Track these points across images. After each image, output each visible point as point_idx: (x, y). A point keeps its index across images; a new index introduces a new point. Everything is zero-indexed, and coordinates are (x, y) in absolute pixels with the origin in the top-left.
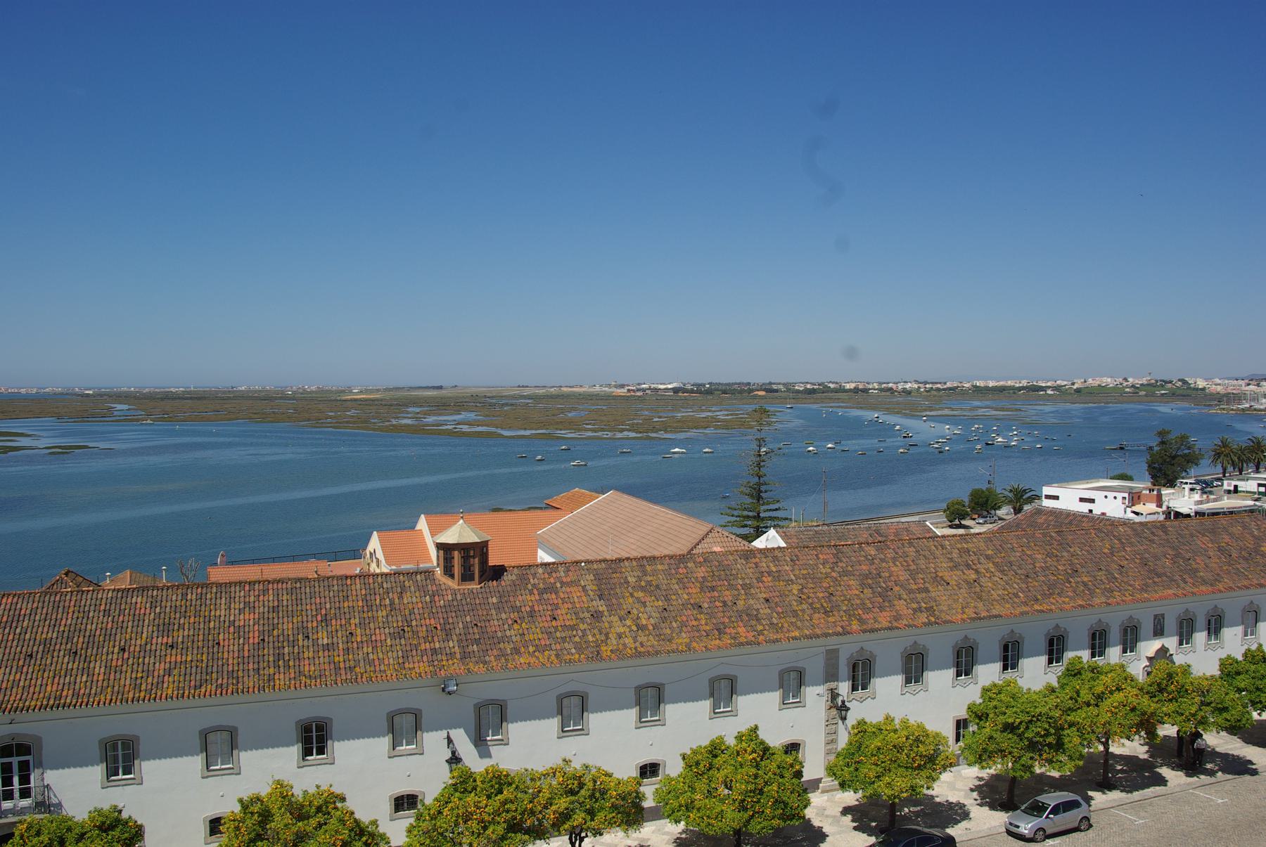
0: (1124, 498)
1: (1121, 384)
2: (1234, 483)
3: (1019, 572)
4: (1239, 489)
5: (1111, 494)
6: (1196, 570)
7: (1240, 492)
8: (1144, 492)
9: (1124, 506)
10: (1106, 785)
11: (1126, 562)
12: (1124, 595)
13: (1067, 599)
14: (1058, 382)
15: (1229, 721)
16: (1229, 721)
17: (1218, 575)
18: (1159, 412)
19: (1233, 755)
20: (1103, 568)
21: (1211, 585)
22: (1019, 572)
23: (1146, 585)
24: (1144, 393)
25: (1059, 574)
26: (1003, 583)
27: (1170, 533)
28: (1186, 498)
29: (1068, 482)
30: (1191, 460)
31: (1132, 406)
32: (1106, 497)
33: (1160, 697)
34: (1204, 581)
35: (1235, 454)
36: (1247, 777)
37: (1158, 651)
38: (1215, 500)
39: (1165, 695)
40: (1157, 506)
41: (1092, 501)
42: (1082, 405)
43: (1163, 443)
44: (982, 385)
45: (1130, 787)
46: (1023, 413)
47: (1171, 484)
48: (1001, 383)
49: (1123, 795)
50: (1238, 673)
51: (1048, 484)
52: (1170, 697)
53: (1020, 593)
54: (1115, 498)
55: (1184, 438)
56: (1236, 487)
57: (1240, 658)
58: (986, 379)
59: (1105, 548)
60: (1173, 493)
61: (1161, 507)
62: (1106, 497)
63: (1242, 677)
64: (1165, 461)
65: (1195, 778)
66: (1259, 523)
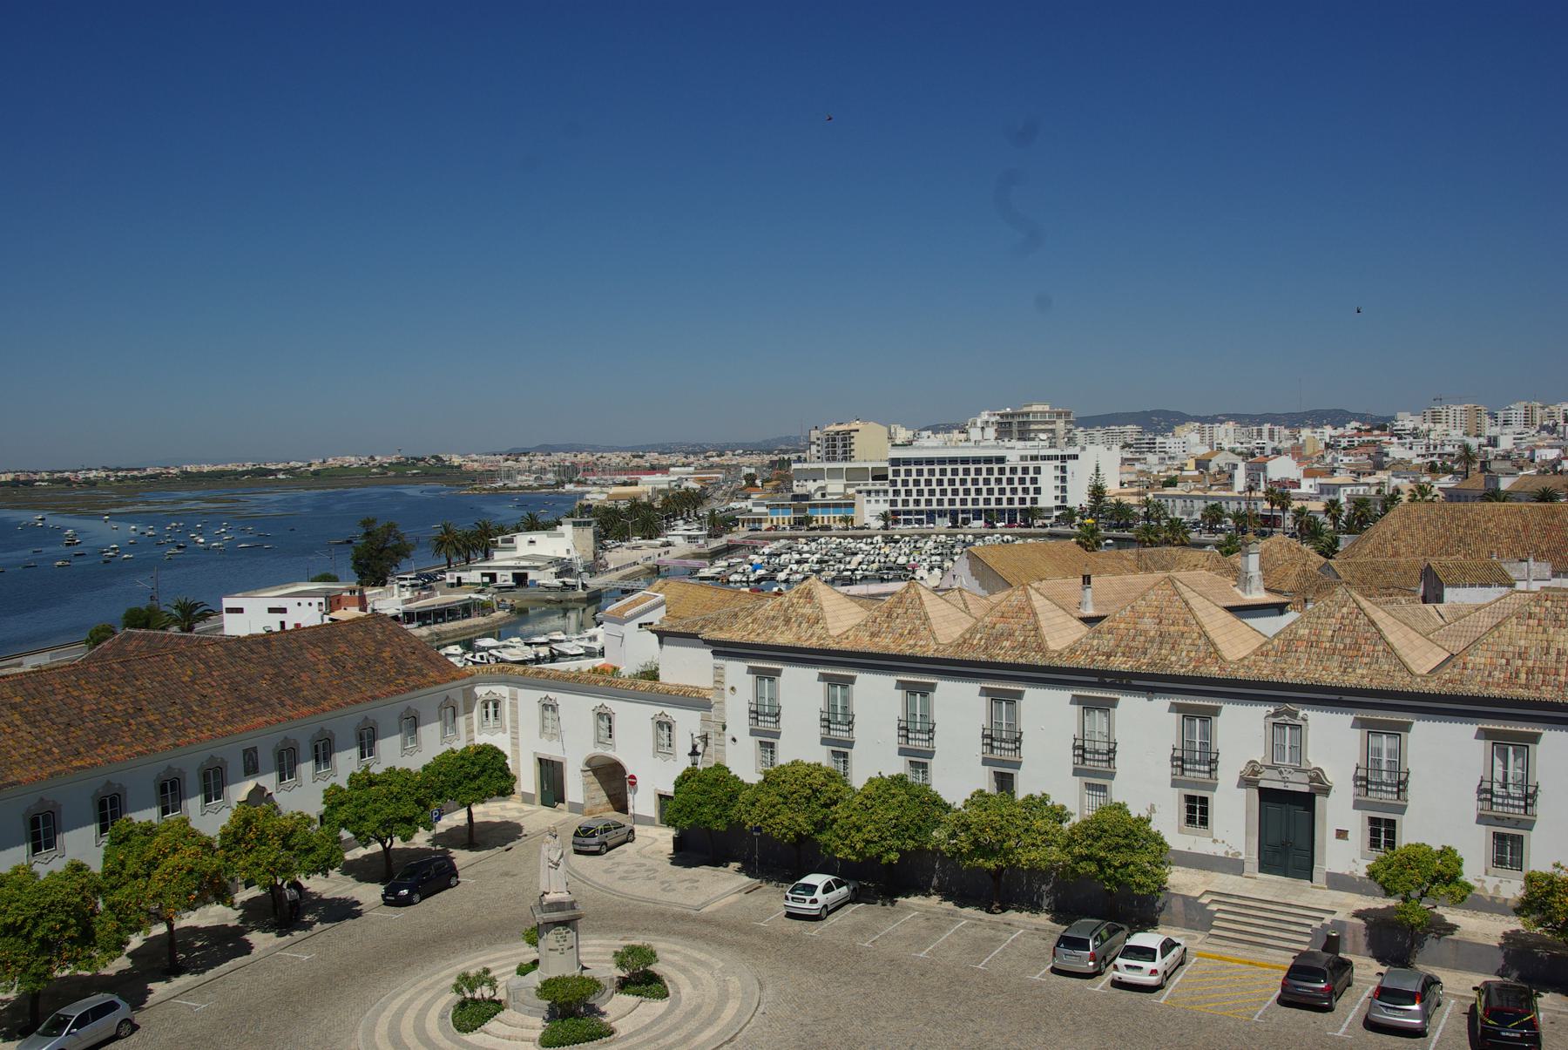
0: (320, 604)
1: (367, 464)
2: (457, 575)
3: (59, 720)
4: (463, 581)
5: (305, 601)
6: (300, 689)
7: (465, 584)
8: (344, 594)
9: (320, 613)
10: (172, 970)
11: (210, 690)
12: (202, 732)
13: (122, 747)
14: (292, 464)
15: (315, 862)
16: (315, 862)
17: (325, 691)
18: (404, 494)
19: (340, 899)
20: (178, 701)
21: (315, 705)
22: (59, 720)
23: (233, 716)
24: (393, 473)
25: (116, 717)
26: (31, 738)
27: (273, 648)
28: (396, 597)
29: (256, 589)
30: (402, 552)
31: (377, 490)
32: (299, 604)
33: (238, 849)
34: (306, 701)
35: (459, 541)
36: (349, 922)
37: (251, 793)
38: (427, 597)
39: (243, 845)
40: (360, 610)
41: (283, 611)
42: (318, 491)
43: (368, 534)
44: (194, 471)
45: (200, 969)
46: (240, 505)
47: (380, 581)
48: (220, 467)
49: (194, 977)
50: (342, 804)
51: (230, 592)
52: (249, 847)
53: (54, 749)
54: (310, 604)
55: (391, 527)
56: (459, 578)
57: (346, 786)
58: (199, 462)
59: (186, 675)
60: (380, 593)
61: (365, 611)
62: (299, 604)
63: (344, 807)
64: (371, 555)
65: (288, 937)
66: (385, 625)
